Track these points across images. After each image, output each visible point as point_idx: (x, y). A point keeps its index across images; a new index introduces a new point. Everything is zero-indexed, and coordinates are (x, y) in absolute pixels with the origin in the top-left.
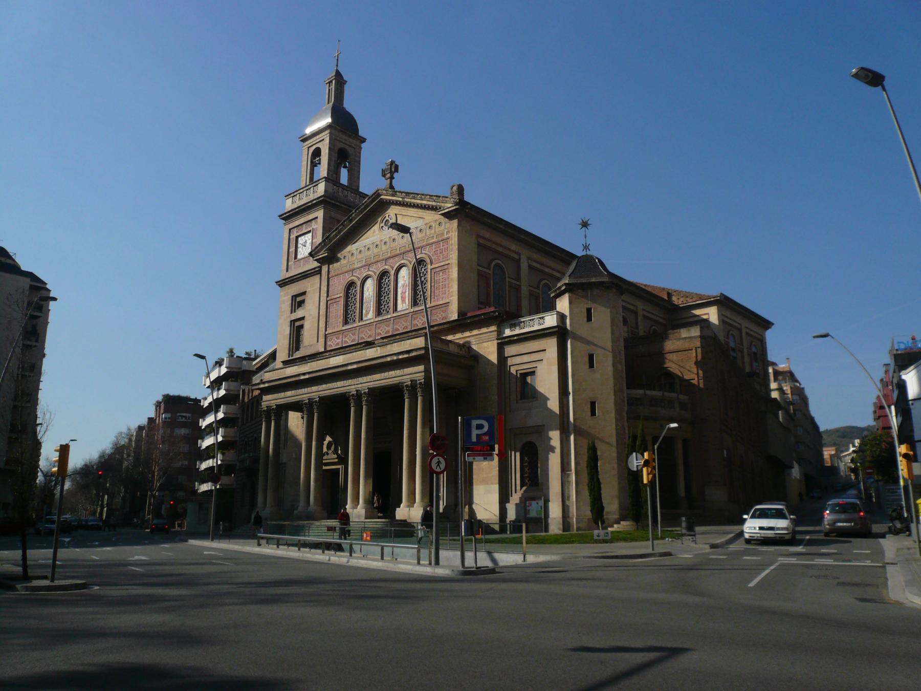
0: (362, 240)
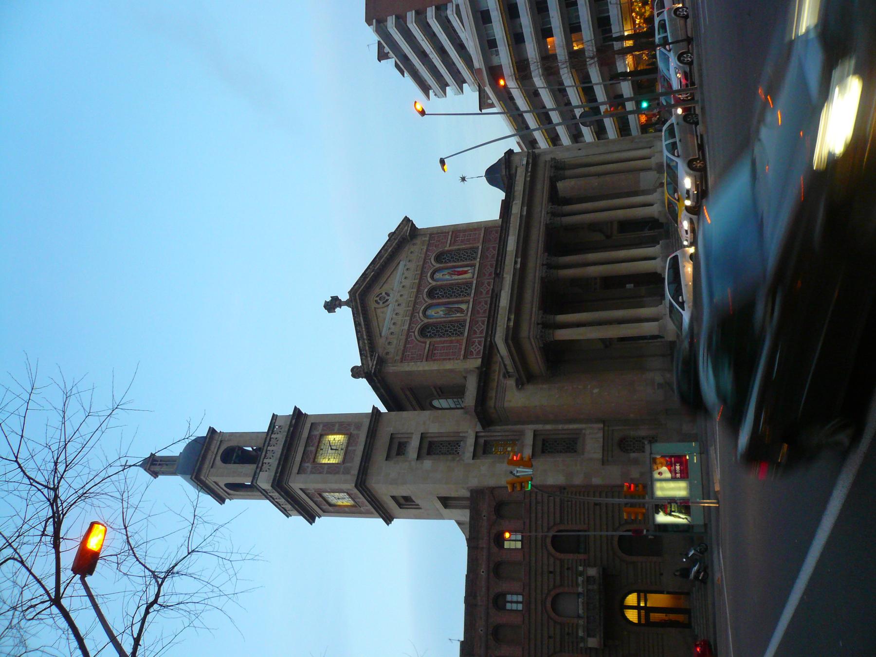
0: (383, 327)
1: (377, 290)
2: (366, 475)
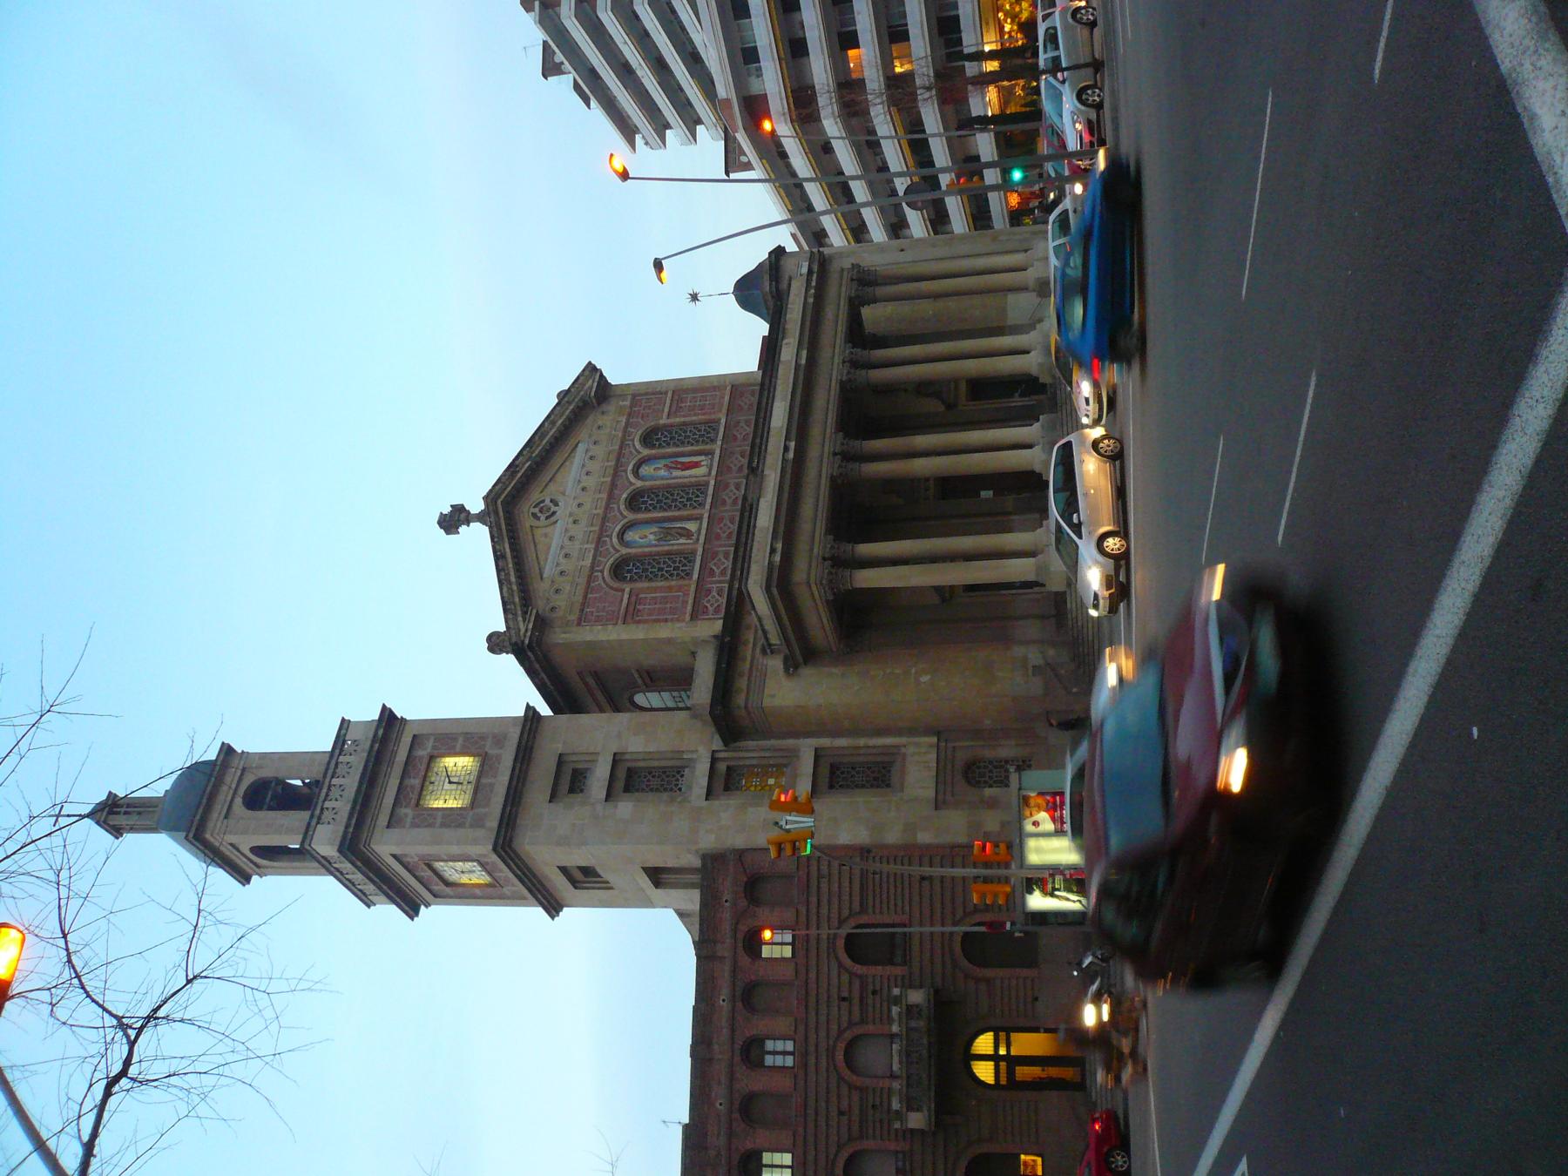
1: (535, 495)
2: (513, 829)
